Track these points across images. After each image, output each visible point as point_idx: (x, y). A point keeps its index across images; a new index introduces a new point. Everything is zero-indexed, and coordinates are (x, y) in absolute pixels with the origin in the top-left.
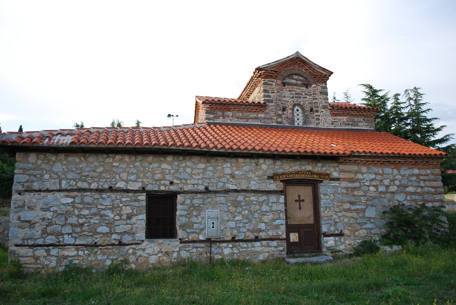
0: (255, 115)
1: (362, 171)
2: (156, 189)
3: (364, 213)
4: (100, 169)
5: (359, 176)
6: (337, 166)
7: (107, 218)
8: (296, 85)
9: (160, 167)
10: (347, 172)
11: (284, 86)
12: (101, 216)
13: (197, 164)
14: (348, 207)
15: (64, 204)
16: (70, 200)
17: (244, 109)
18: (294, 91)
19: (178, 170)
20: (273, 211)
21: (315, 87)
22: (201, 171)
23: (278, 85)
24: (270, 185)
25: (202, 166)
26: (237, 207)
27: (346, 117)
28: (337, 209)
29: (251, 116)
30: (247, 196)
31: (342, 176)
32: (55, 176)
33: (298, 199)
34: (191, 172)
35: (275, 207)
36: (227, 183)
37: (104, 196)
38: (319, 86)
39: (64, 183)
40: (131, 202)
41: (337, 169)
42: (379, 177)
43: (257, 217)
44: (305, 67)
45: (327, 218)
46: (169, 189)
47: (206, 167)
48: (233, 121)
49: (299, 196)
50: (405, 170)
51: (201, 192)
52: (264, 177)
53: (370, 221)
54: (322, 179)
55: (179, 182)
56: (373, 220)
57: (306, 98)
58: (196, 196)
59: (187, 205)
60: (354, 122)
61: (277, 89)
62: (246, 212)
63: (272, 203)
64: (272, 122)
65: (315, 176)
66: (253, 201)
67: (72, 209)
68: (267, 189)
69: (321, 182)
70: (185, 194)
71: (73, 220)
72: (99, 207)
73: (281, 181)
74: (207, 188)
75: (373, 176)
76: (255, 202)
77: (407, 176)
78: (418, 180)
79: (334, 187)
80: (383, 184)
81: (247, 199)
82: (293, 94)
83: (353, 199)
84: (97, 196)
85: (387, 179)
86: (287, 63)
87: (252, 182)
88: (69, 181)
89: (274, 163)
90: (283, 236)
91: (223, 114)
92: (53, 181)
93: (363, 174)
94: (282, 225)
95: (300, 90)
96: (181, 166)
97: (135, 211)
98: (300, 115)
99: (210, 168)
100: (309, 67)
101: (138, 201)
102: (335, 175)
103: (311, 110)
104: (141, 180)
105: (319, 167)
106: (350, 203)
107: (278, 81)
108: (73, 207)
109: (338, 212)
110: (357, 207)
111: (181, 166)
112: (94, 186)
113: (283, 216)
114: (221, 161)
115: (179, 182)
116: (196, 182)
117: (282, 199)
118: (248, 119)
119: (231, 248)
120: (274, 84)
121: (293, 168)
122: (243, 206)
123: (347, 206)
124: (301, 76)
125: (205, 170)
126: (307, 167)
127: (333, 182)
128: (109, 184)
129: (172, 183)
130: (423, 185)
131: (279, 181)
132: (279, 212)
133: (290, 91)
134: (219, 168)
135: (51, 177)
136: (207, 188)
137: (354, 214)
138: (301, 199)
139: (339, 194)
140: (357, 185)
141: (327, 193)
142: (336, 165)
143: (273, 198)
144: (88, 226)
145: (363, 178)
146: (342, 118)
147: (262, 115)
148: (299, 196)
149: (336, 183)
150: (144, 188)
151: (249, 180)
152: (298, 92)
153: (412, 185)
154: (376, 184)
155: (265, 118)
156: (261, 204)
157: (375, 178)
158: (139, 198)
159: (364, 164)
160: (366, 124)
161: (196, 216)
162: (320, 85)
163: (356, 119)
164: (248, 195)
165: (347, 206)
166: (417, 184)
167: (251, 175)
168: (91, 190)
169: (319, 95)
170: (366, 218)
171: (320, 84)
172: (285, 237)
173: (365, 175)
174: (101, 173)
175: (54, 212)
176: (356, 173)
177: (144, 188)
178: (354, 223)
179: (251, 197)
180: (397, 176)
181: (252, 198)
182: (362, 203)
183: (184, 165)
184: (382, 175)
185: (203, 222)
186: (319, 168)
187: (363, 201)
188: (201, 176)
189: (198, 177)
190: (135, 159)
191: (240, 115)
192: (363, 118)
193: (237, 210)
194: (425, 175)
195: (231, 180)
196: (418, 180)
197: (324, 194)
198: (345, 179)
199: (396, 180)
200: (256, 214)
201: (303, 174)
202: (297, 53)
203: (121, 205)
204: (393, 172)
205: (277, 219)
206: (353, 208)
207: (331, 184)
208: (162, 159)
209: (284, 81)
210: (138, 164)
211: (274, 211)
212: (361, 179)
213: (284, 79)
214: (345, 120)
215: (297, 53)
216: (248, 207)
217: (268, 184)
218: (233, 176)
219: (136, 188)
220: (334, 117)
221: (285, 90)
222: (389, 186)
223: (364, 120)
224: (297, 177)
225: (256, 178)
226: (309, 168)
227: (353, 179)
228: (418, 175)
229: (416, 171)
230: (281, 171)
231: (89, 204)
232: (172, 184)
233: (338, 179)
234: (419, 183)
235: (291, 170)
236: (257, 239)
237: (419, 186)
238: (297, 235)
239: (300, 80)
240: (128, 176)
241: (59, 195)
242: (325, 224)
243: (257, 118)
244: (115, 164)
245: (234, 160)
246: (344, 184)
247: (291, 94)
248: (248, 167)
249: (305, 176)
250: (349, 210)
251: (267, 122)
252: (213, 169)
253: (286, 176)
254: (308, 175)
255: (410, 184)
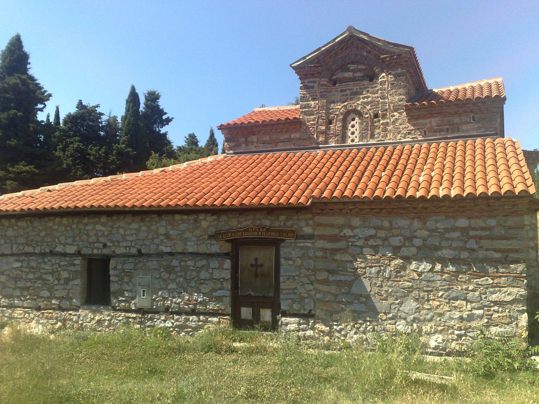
0: (286, 136)
1: (353, 224)
2: (90, 252)
3: (350, 287)
4: (43, 234)
5: (348, 232)
6: (310, 219)
7: (48, 282)
8: (354, 79)
9: (94, 228)
10: (326, 225)
11: (335, 84)
12: (44, 280)
13: (131, 224)
14: (325, 277)
15: (15, 268)
16: (18, 265)
17: (271, 130)
18: (349, 90)
19: (111, 231)
20: (214, 279)
21: (383, 77)
22: (133, 232)
23: (323, 85)
24: (212, 246)
25: (135, 226)
26: (170, 273)
27: (438, 119)
28: (305, 280)
29: (282, 138)
30: (183, 261)
31: (319, 231)
32: (8, 241)
33: (254, 263)
34: (125, 233)
35: (217, 274)
36: (161, 245)
37: (46, 260)
38: (390, 74)
39: (15, 247)
40: (68, 266)
41: (311, 222)
42: (382, 234)
43: (194, 285)
44: (366, 48)
45: (288, 291)
46: (101, 252)
47: (140, 227)
48: (258, 148)
49: (256, 259)
50: (437, 221)
51: (134, 256)
52: (204, 237)
53: (359, 300)
54: (284, 237)
55: (111, 245)
56: (364, 300)
57: (368, 97)
58: (128, 260)
59: (118, 270)
60: (452, 125)
61: (321, 92)
62: (181, 279)
63: (213, 269)
64: (311, 144)
65: (273, 234)
66: (190, 266)
67: (20, 273)
68: (207, 252)
69: (283, 241)
70: (117, 257)
71: (21, 284)
72: (42, 271)
73: (227, 241)
74: (139, 251)
75: (372, 232)
76: (191, 268)
77: (440, 230)
78: (463, 238)
79: (302, 248)
80: (389, 243)
81: (183, 263)
82: (347, 95)
83: (333, 266)
84: (40, 260)
85: (398, 235)
86: (335, 48)
87: (189, 243)
88: (18, 245)
89: (218, 219)
90: (227, 311)
91: (246, 140)
92: (7, 245)
93: (353, 228)
94: (226, 297)
95: (358, 87)
96: (114, 226)
97: (71, 276)
98: (357, 126)
99: (144, 228)
100: (372, 46)
101: (74, 265)
102: (307, 230)
103: (376, 116)
104: (77, 243)
105: (281, 221)
106: (328, 271)
107: (323, 79)
108: (21, 271)
109: (306, 284)
110: (338, 278)
111: (114, 226)
112: (37, 251)
113: (228, 285)
114: (156, 219)
115: (111, 245)
116: (129, 244)
117: (228, 264)
118: (278, 143)
119: (163, 320)
120: (316, 85)
121: (243, 224)
122: (177, 272)
123: (324, 275)
124: (361, 64)
125: (138, 230)
126: (263, 221)
127: (301, 241)
128: (50, 248)
129: (105, 246)
130: (475, 246)
131: (224, 241)
132: (222, 280)
133: (342, 91)
134: (153, 228)
135: (6, 243)
136: (139, 251)
137: (333, 289)
138: (259, 263)
139: (310, 258)
140: (341, 245)
141: (291, 256)
142: (309, 216)
143: (214, 263)
144: (33, 289)
145: (352, 234)
146: (427, 121)
147: (297, 135)
148: (256, 259)
149: (306, 242)
150: (79, 252)
151: (185, 241)
152: (354, 91)
153: (451, 246)
154: (374, 244)
155: (299, 139)
156: (199, 270)
157: (376, 235)
158: (75, 262)
159: (357, 214)
160: (476, 126)
161: (127, 283)
162: (393, 72)
163: (456, 120)
164: (184, 259)
165: (324, 275)
166: (461, 244)
167: (188, 235)
168: (35, 254)
169: (389, 89)
170: (352, 294)
171: (393, 71)
172: (230, 312)
173: (357, 231)
174: (43, 237)
175: (8, 275)
176: (341, 227)
177: (79, 252)
178: (332, 301)
179: (187, 261)
180: (419, 231)
181: (189, 263)
182: (348, 272)
183: (117, 226)
184: (391, 228)
185: (134, 289)
186: (280, 222)
187: (349, 270)
188: (134, 237)
189: (131, 239)
190: (73, 221)
191: (268, 138)
192: (471, 116)
193: (171, 278)
194: (483, 229)
195: (165, 241)
196: (463, 238)
197: (286, 259)
198: (322, 237)
199: (416, 237)
200: (193, 282)
201: (255, 231)
202: (350, 29)
203: (59, 269)
204: (412, 224)
205: (220, 289)
206: (331, 278)
207: (298, 245)
208: (97, 220)
209: (334, 77)
210: (74, 226)
211: (216, 279)
212: (350, 237)
213: (333, 74)
214: (434, 124)
215: (350, 29)
216: (183, 274)
217: (208, 246)
218: (168, 236)
219: (72, 252)
220: (412, 122)
221: (335, 91)
222: (400, 247)
223: (474, 120)
224: (246, 235)
225: (194, 239)
226: (267, 223)
227: (336, 236)
228: (464, 230)
229: (462, 222)
230: (227, 227)
231: (33, 268)
232: (105, 247)
233: (311, 237)
234: (466, 242)
235: (239, 226)
236: (193, 312)
237: (465, 249)
238: (250, 310)
239: (360, 70)
240: (66, 239)
241: (11, 259)
242: (285, 300)
243: (289, 140)
244: (55, 227)
245: (170, 216)
246: (320, 244)
247: (343, 95)
248: (185, 225)
249: (258, 233)
250: (326, 282)
251: (304, 144)
252: (147, 229)
253: (232, 234)
254: (262, 232)
255: (444, 244)
